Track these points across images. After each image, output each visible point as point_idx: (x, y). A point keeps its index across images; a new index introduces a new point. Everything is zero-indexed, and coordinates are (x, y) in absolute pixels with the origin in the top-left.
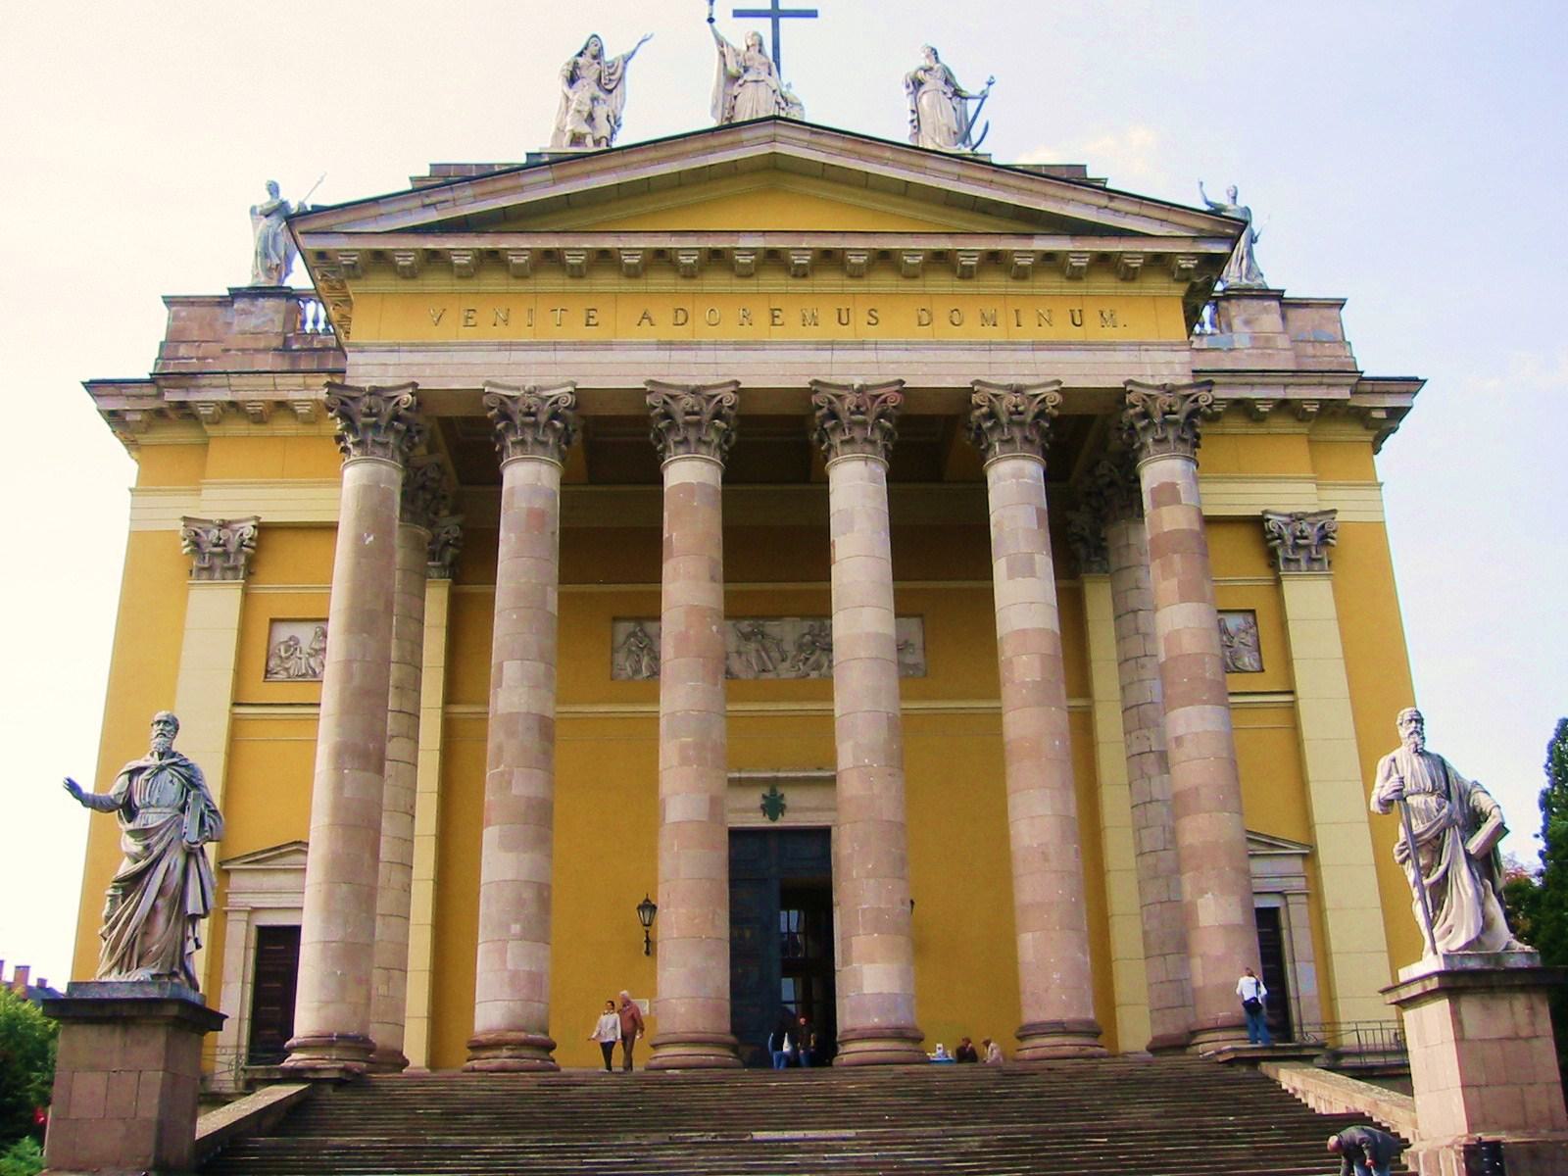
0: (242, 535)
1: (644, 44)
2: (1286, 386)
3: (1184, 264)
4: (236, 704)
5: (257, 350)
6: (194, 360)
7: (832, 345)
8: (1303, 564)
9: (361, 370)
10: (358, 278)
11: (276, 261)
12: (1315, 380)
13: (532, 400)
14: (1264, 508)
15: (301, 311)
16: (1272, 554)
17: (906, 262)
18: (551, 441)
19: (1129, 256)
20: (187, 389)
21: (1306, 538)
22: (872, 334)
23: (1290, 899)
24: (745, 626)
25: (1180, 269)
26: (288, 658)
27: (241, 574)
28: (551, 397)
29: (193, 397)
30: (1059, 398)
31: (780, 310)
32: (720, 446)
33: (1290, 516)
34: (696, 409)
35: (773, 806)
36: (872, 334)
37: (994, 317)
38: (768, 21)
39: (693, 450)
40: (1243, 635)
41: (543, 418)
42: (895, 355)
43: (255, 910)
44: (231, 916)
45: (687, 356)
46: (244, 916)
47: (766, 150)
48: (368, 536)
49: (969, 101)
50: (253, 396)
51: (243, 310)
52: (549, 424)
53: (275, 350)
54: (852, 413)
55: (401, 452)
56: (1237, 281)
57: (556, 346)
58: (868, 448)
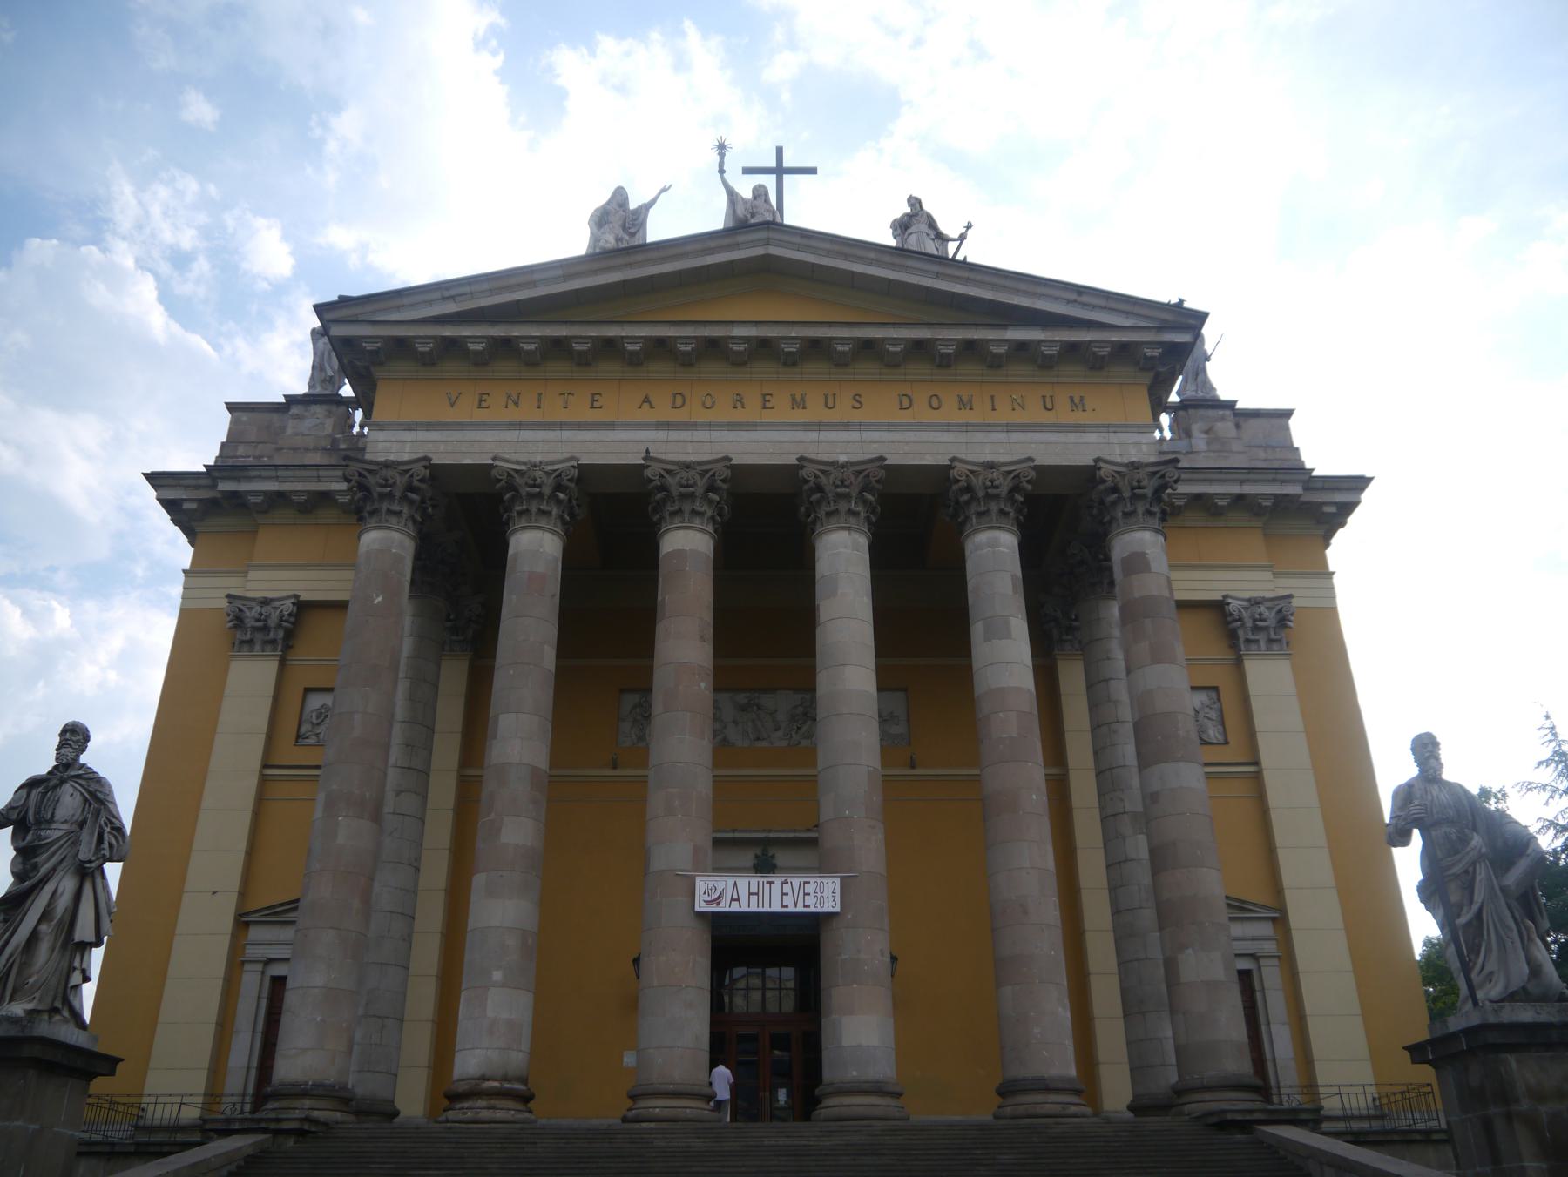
0: (282, 611)
1: (662, 195)
2: (1242, 482)
3: (1149, 353)
4: (265, 766)
6: (251, 459)
7: (819, 426)
8: (1263, 644)
9: (380, 446)
10: (381, 364)
11: (330, 373)
12: (1270, 477)
13: (538, 474)
14: (1224, 593)
15: (350, 416)
17: (888, 351)
18: (555, 512)
19: (1097, 345)
20: (238, 479)
21: (1265, 620)
22: (857, 416)
23: (1262, 962)
24: (742, 698)
25: (1146, 358)
26: (319, 724)
27: (280, 647)
28: (555, 471)
29: (244, 487)
30: (1033, 474)
31: (771, 395)
32: (712, 518)
33: (1249, 600)
34: (691, 482)
36: (857, 416)
37: (970, 402)
38: (773, 177)
39: (686, 519)
40: (1207, 710)
41: (547, 490)
42: (876, 435)
43: (269, 962)
44: (247, 967)
45: (685, 435)
46: (259, 967)
47: (760, 251)
48: (378, 596)
49: (950, 244)
50: (299, 487)
51: (297, 415)
52: (553, 497)
53: (325, 449)
54: (837, 487)
55: (415, 521)
56: (1194, 393)
57: (562, 426)
58: (852, 520)
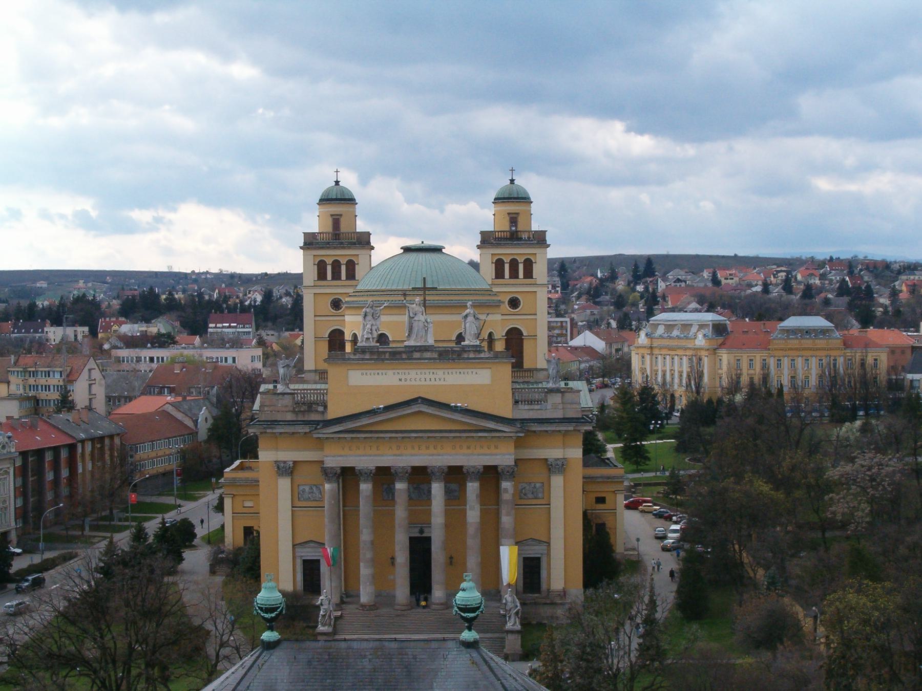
4: (293, 507)
5: (287, 412)
7: (433, 455)
13: (366, 471)
16: (550, 469)
35: (421, 532)
47: (417, 410)
